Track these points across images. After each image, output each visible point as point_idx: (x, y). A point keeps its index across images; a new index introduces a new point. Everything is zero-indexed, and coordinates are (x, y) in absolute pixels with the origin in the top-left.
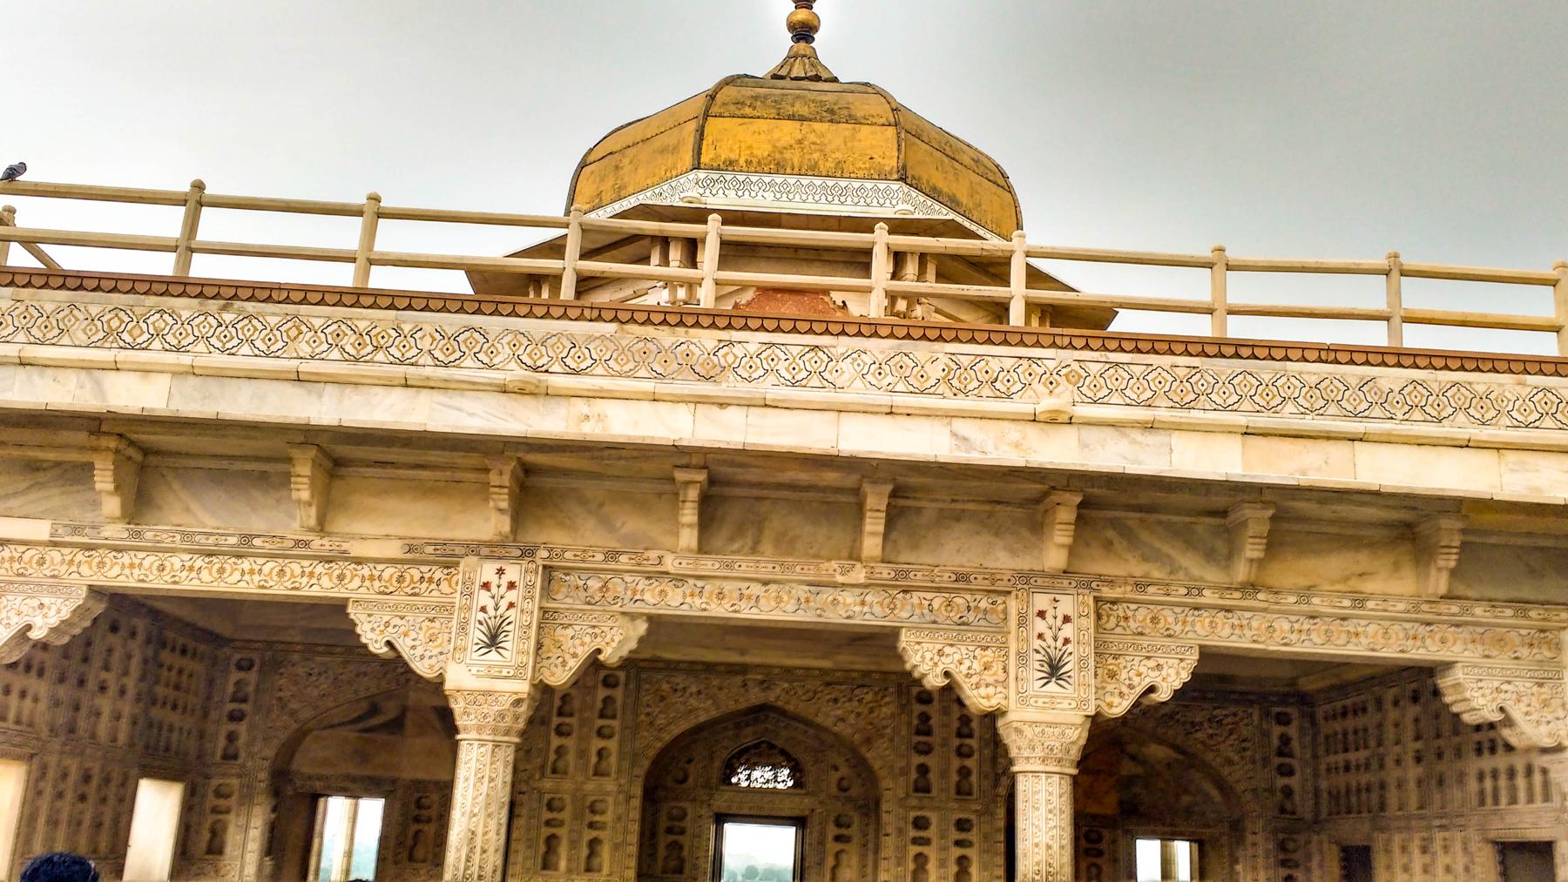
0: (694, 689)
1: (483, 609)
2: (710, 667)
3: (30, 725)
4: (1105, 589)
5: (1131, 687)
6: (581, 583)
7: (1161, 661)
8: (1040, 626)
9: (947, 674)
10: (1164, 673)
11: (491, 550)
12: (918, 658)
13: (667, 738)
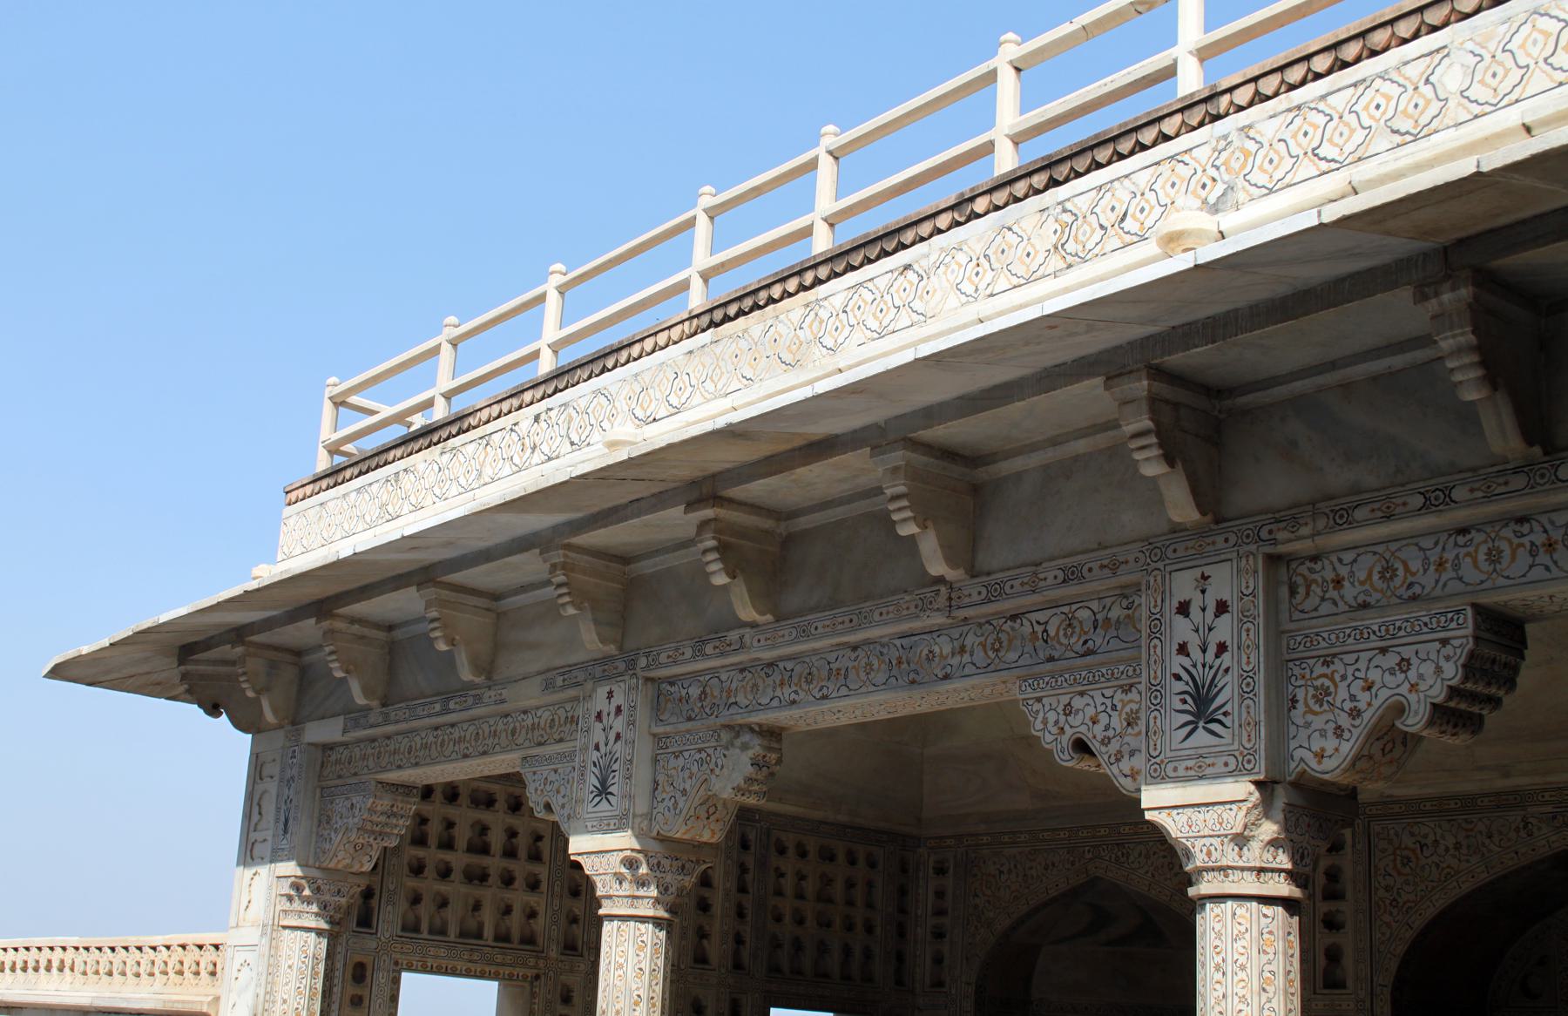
0: (1451, 841)
1: (597, 748)
2: (1468, 803)
3: (529, 940)
4: (1281, 536)
5: (1355, 713)
6: (684, 692)
7: (1407, 652)
8: (1182, 629)
9: (1081, 747)
10: (1412, 674)
11: (602, 670)
12: (1039, 725)
13: (1419, 923)
